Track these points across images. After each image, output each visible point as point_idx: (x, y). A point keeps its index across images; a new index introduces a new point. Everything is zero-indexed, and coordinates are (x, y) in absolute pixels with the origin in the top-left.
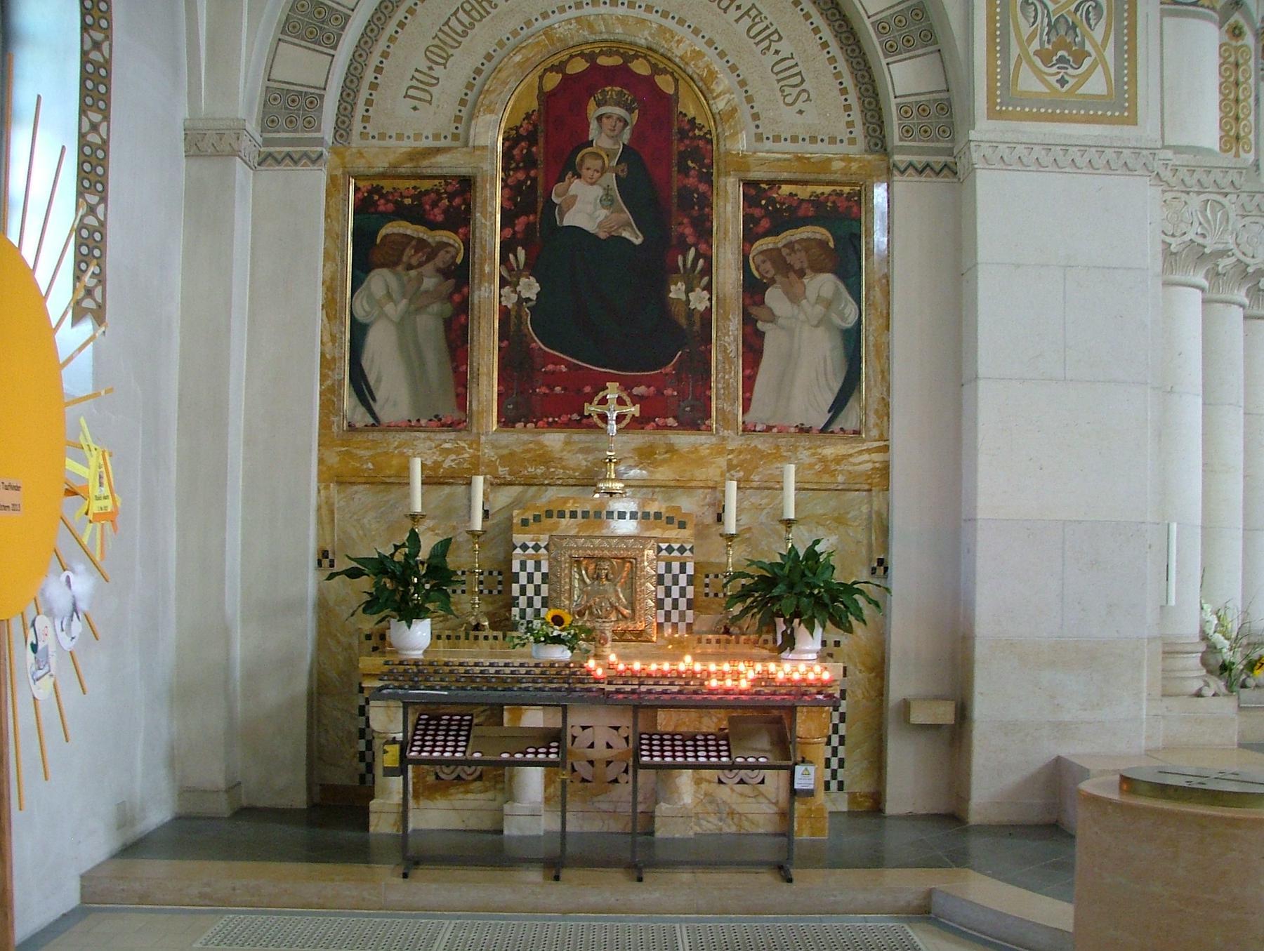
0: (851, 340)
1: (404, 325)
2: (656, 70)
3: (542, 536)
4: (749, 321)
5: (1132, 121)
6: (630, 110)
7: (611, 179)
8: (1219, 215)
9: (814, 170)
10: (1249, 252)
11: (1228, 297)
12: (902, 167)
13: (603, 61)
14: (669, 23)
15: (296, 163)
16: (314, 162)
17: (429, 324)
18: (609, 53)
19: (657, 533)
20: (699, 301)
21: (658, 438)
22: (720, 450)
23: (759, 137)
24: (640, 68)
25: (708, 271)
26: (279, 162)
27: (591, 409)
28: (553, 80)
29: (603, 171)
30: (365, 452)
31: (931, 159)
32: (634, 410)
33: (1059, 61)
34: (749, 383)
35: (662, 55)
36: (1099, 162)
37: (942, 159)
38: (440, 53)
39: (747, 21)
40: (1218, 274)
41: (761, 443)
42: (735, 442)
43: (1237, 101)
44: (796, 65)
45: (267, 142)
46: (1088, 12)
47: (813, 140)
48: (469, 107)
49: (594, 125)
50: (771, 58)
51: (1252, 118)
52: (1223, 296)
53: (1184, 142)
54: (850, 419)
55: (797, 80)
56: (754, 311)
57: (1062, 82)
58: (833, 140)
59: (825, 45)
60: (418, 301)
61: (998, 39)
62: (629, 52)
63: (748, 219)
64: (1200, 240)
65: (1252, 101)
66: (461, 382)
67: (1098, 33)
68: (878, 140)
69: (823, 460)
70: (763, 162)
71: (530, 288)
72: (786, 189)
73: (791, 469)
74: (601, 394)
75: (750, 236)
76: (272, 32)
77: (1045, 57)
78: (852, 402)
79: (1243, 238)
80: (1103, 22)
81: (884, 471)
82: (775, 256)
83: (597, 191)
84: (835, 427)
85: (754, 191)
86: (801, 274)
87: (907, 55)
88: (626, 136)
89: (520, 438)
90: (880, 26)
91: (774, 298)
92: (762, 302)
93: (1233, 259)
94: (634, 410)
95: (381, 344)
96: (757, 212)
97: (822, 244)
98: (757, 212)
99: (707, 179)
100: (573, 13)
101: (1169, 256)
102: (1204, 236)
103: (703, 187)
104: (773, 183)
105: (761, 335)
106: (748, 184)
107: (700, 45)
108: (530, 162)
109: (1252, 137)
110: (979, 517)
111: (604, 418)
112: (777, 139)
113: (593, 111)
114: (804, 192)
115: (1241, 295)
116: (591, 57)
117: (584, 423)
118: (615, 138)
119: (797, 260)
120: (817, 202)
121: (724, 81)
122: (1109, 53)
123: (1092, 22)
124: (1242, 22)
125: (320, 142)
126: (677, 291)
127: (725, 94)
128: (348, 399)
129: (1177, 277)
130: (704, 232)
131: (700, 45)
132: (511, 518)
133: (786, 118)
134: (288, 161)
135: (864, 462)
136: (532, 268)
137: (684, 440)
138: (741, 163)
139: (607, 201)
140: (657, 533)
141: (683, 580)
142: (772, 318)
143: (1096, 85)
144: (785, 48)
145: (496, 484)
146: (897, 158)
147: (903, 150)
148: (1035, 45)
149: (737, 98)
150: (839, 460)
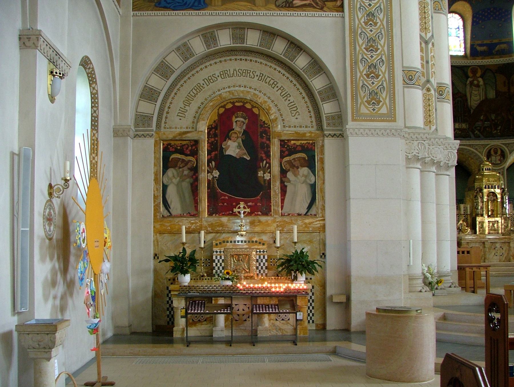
0: (313, 187)
1: (178, 185)
2: (253, 107)
3: (222, 249)
4: (282, 182)
5: (395, 121)
6: (245, 119)
7: (240, 140)
8: (423, 147)
9: (300, 136)
10: (435, 156)
11: (429, 170)
12: (327, 135)
13: (237, 104)
15: (145, 137)
16: (151, 137)
17: (186, 185)
18: (239, 102)
19: (256, 247)
20: (267, 176)
21: (256, 218)
22: (274, 221)
23: (284, 126)
24: (248, 106)
25: (269, 167)
26: (140, 137)
27: (236, 210)
28: (222, 110)
29: (238, 137)
30: (167, 224)
31: (336, 132)
32: (248, 210)
33: (372, 104)
34: (283, 201)
35: (255, 102)
36: (385, 134)
37: (339, 132)
38: (188, 102)
39: (280, 91)
40: (426, 163)
41: (286, 219)
42: (279, 219)
43: (429, 110)
44: (295, 104)
45: (136, 131)
46: (381, 89)
47: (301, 127)
48: (197, 119)
49: (234, 124)
50: (287, 102)
51: (434, 115)
52: (427, 170)
53: (412, 125)
54: (313, 211)
55: (295, 109)
56: (283, 179)
57: (374, 110)
58: (306, 127)
59: (304, 98)
60: (182, 178)
61: (354, 97)
62: (245, 101)
63: (281, 152)
64: (417, 155)
65: (434, 110)
66: (196, 202)
67: (384, 95)
68: (320, 127)
69: (305, 224)
70: (285, 134)
71: (216, 173)
72: (292, 142)
73: (295, 227)
74: (239, 206)
75: (282, 157)
76: (137, 97)
77: (368, 102)
78: (314, 206)
79: (433, 152)
80: (385, 92)
81: (324, 227)
82: (289, 162)
83: (236, 144)
84: (309, 214)
85: (283, 143)
86: (298, 168)
87: (328, 101)
88: (244, 127)
89: (214, 219)
90: (320, 93)
91: (290, 175)
92: (286, 177)
93: (430, 158)
94: (248, 210)
95: (172, 191)
96: (284, 149)
97: (304, 158)
98: (284, 149)
99: (269, 139)
100: (228, 90)
101: (408, 159)
102: (418, 153)
103: (268, 142)
104: (288, 140)
105: (286, 186)
106: (281, 141)
107: (266, 99)
108: (215, 135)
109: (434, 121)
110: (351, 240)
111: (239, 212)
112: (290, 127)
113: (234, 119)
114: (298, 143)
115: (434, 169)
116: (233, 103)
117: (234, 215)
118: (241, 128)
119: (297, 163)
120: (302, 146)
121: (273, 110)
122: (387, 101)
123: (382, 92)
124: (430, 87)
125: (152, 130)
126: (260, 174)
128: (162, 208)
129: (411, 166)
130: (268, 156)
131: (266, 99)
132: (212, 243)
133: (293, 121)
134: (143, 136)
135: (318, 224)
136: (217, 168)
137: (263, 219)
138: (279, 135)
139: (239, 147)
140: (256, 247)
141: (264, 261)
142: (289, 181)
143: (384, 110)
144: (292, 99)
145: (207, 233)
146: (326, 132)
147: (327, 130)
148: (365, 99)
149: (278, 115)
150: (310, 224)
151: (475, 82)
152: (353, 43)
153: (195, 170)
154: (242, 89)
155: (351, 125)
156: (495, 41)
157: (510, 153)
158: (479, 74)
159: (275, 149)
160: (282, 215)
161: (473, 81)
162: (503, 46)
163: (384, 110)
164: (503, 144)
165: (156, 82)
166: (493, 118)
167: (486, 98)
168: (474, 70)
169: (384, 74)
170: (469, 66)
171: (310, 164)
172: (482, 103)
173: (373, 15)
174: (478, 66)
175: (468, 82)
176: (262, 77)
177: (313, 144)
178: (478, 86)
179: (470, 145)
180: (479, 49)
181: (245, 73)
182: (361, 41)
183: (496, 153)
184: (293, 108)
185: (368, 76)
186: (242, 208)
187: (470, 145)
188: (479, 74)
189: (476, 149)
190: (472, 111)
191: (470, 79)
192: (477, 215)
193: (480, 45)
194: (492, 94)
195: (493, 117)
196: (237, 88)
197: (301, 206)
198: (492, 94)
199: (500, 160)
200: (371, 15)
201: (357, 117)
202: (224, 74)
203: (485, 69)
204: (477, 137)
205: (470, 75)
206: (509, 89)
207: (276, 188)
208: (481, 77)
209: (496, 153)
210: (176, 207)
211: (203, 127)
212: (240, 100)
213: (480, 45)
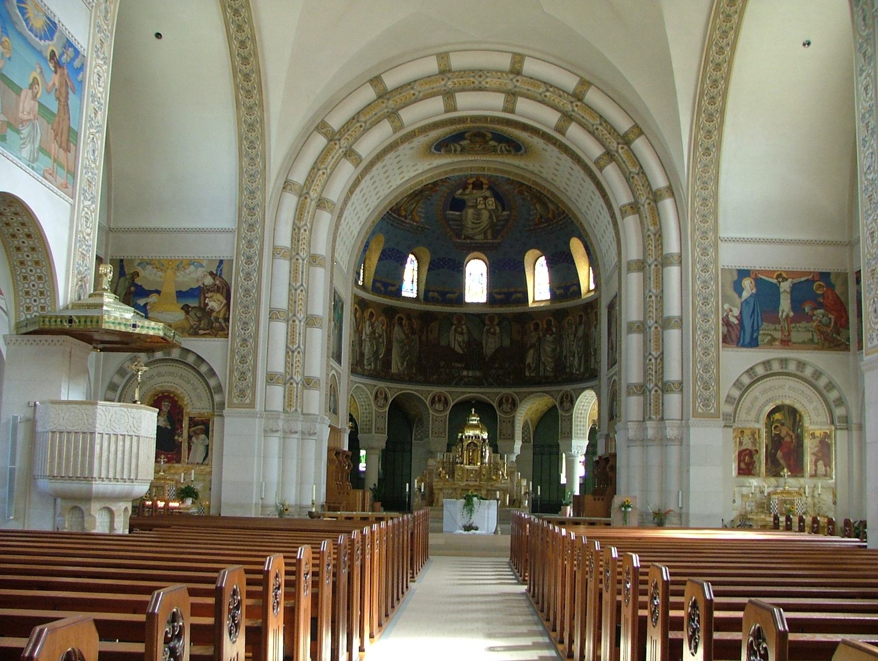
4: (189, 443)
5: (254, 408)
14: (178, 387)
20: (180, 439)
24: (172, 395)
28: (156, 398)
32: (166, 460)
34: (189, 454)
41: (190, 466)
54: (206, 462)
61: (230, 393)
62: (169, 392)
73: (193, 471)
75: (190, 428)
76: (104, 389)
82: (194, 431)
83: (163, 419)
85: (191, 419)
90: (213, 388)
91: (193, 439)
94: (166, 460)
101: (265, 431)
107: (183, 391)
113: (163, 403)
120: (202, 421)
122: (250, 395)
126: (176, 438)
131: (183, 391)
133: (198, 405)
135: (208, 470)
137: (176, 465)
138: (188, 414)
139: (164, 421)
144: (198, 391)
149: (189, 401)
151: (492, 330)
152: (232, 358)
154: (169, 384)
155: (227, 411)
156: (512, 290)
157: (520, 402)
158: (495, 323)
159: (185, 423)
160: (188, 463)
161: (490, 329)
162: (519, 295)
163: (248, 401)
164: (515, 392)
165: (117, 379)
166: (507, 366)
167: (501, 346)
168: (492, 317)
169: (250, 378)
170: (486, 314)
171: (207, 432)
172: (497, 351)
173: (246, 340)
174: (497, 314)
175: (485, 329)
177: (209, 420)
178: (494, 334)
179: (482, 393)
180: (496, 296)
181: (171, 374)
182: (237, 357)
183: (507, 401)
184: (199, 397)
185: (239, 379)
187: (482, 393)
188: (495, 323)
189: (489, 397)
190: (487, 359)
191: (487, 327)
192: (457, 463)
193: (500, 294)
194: (507, 342)
195: (507, 365)
196: (166, 384)
197: (199, 457)
198: (507, 342)
199: (510, 408)
200: (245, 340)
203: (502, 317)
204: (490, 385)
205: (487, 322)
206: (522, 338)
207: (185, 446)
208: (498, 325)
209: (507, 401)
212: (167, 391)
213: (500, 294)
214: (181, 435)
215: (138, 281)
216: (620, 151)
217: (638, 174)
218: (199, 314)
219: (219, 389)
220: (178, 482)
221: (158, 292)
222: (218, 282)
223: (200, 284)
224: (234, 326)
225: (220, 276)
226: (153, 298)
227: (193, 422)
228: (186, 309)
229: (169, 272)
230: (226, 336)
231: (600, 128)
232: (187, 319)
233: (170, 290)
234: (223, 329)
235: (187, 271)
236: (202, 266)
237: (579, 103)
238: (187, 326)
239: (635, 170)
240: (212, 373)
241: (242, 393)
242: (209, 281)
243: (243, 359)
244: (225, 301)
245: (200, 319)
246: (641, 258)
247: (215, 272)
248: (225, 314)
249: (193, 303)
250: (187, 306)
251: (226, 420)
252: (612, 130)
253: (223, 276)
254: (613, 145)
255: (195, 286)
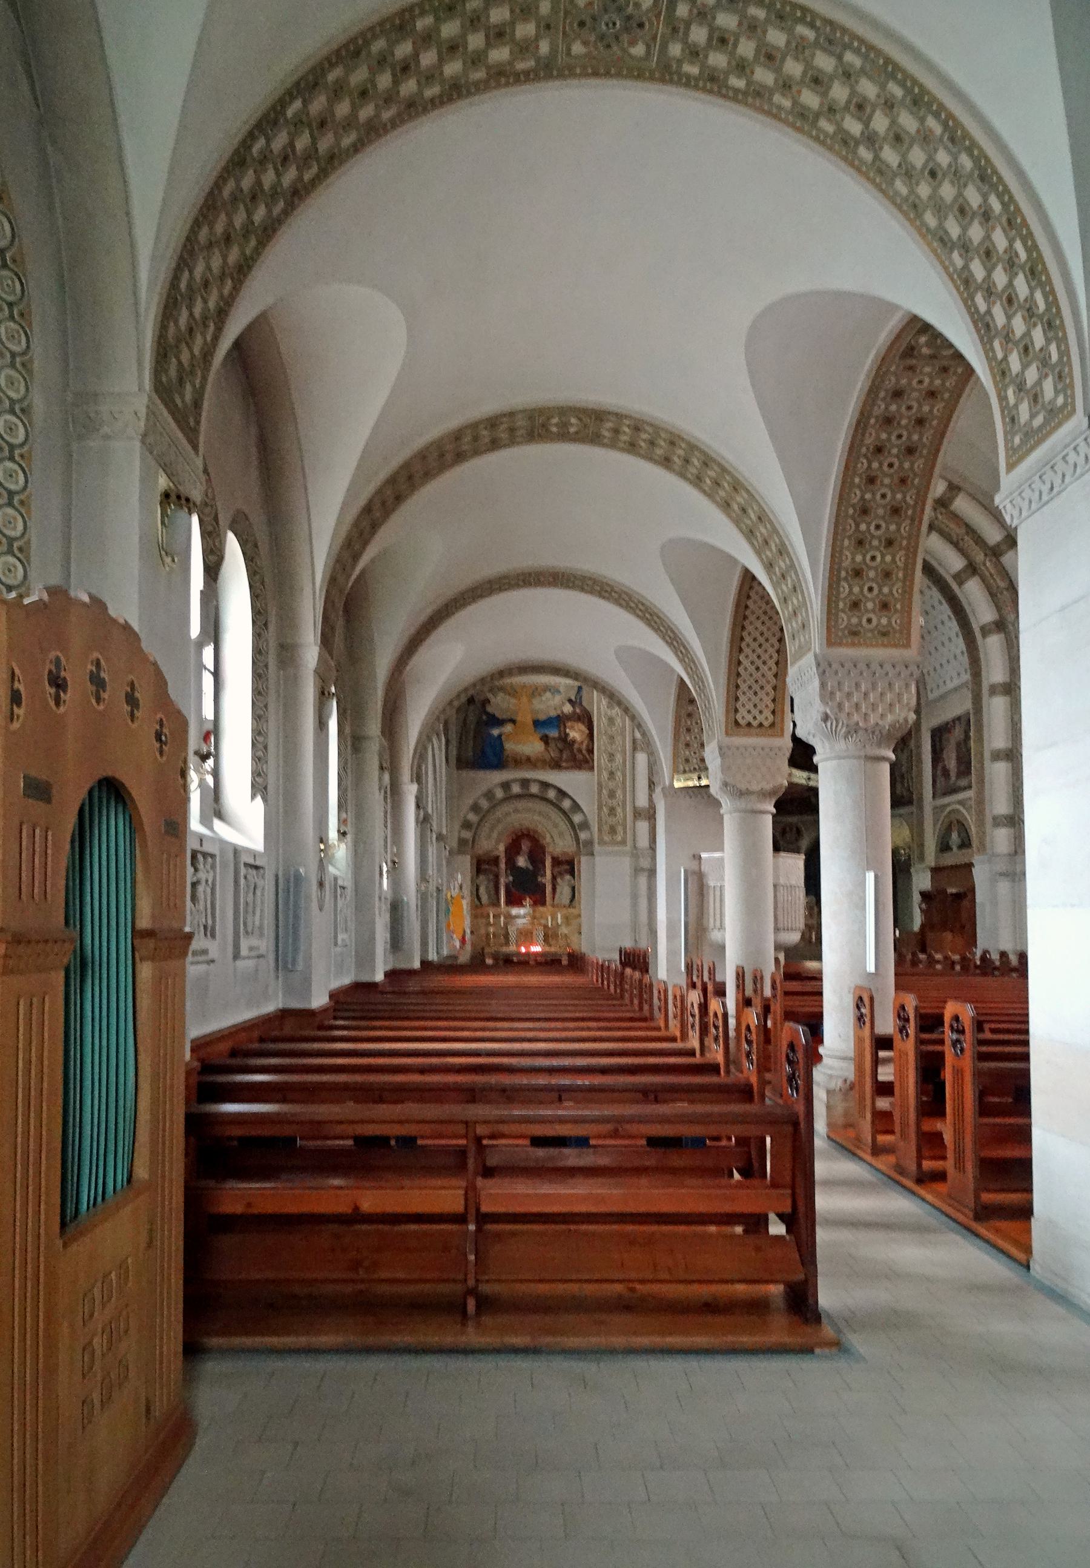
0: (573, 889)
1: (487, 888)
9: (565, 853)
17: (492, 884)
30: (479, 911)
38: (492, 829)
48: (498, 842)
60: (489, 880)
61: (600, 830)
62: (528, 830)
66: (498, 899)
71: (511, 878)
85: (553, 859)
91: (559, 880)
95: (482, 890)
121: (548, 836)
127: (548, 839)
143: (619, 838)
153: (497, 877)
155: (597, 848)
159: (548, 863)
165: (473, 817)
171: (572, 873)
176: (540, 813)
181: (529, 810)
183: (791, 830)
184: (561, 834)
186: (528, 901)
197: (566, 900)
200: (612, 774)
201: (602, 842)
202: (516, 811)
209: (791, 830)
210: (485, 898)
211: (502, 848)
214: (544, 875)
215: (489, 709)
216: (988, 564)
217: (1007, 589)
218: (560, 745)
219: (585, 825)
220: (546, 927)
221: (513, 721)
222: (578, 711)
223: (559, 712)
224: (599, 757)
225: (581, 703)
226: (508, 728)
227: (556, 862)
228: (545, 739)
229: (524, 699)
230: (592, 768)
231: (966, 537)
232: (546, 749)
233: (525, 719)
234: (587, 762)
235: (544, 698)
236: (559, 692)
237: (944, 511)
238: (548, 759)
239: (1002, 585)
240: (576, 807)
241: (613, 830)
242: (568, 709)
243: (612, 795)
244: (587, 732)
245: (561, 751)
246: (1008, 680)
247: (573, 698)
248: (588, 746)
249: (553, 733)
250: (546, 736)
251: (597, 858)
252: (979, 540)
253: (584, 704)
254: (979, 557)
255: (553, 714)
